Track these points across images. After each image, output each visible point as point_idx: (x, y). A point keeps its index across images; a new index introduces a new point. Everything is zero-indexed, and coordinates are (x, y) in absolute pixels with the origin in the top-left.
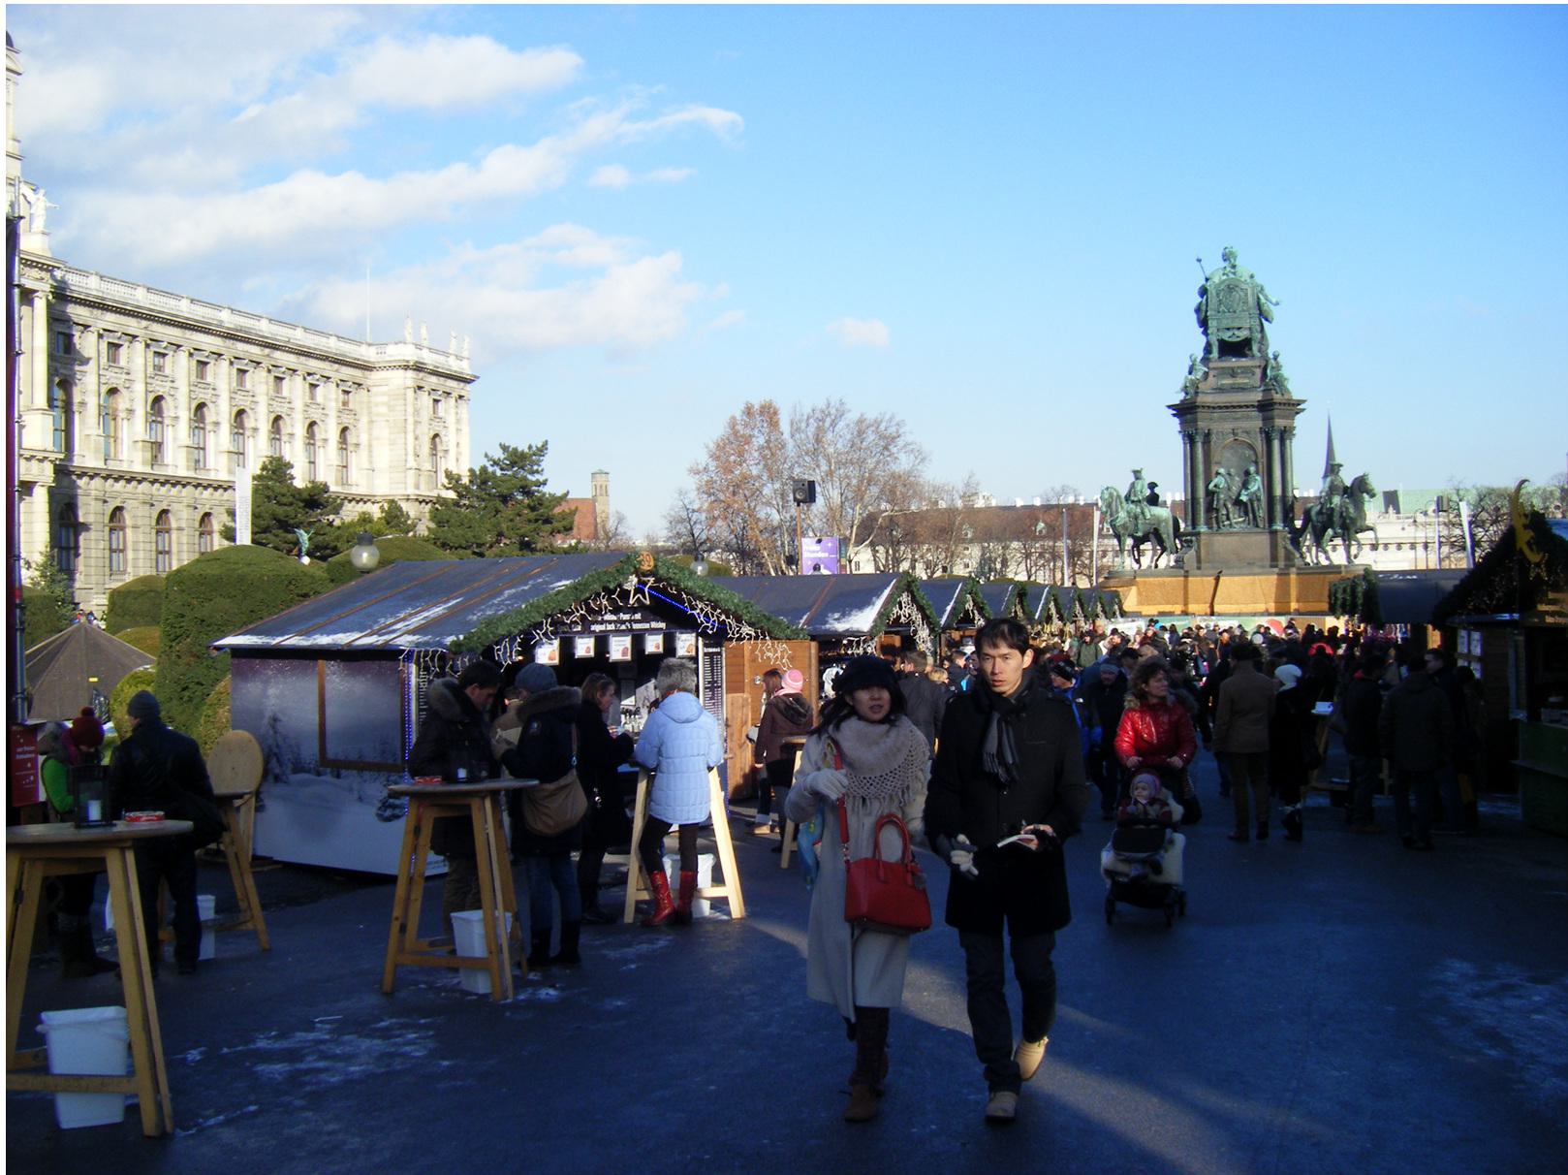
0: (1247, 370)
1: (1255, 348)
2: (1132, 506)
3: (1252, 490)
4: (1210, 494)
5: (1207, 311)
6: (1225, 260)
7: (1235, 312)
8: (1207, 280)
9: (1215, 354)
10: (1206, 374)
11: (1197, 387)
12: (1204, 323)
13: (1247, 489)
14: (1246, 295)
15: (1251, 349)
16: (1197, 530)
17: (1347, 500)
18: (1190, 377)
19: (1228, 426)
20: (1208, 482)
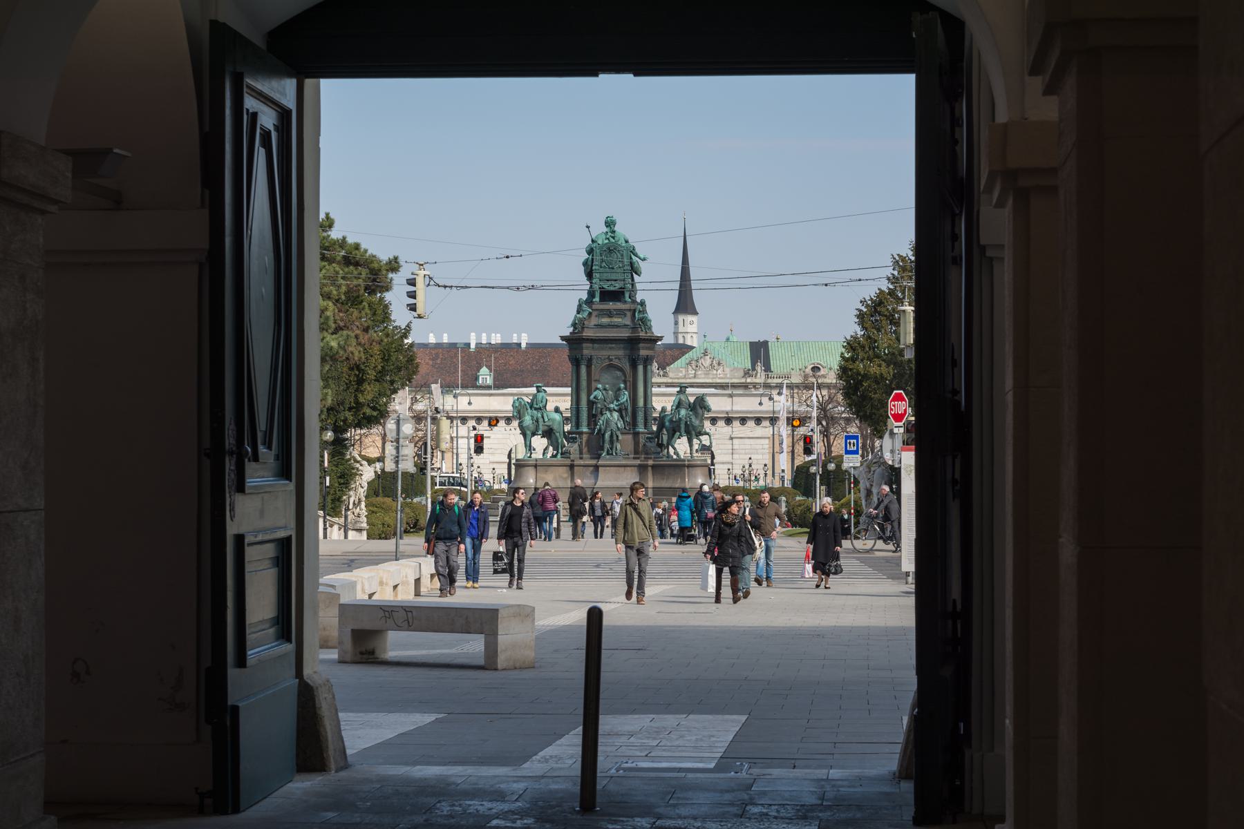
0: (621, 313)
1: (627, 295)
2: (535, 412)
3: (622, 401)
4: (591, 404)
5: (592, 266)
6: (607, 227)
7: (613, 268)
8: (593, 241)
9: (597, 299)
10: (590, 314)
11: (584, 324)
12: (589, 275)
13: (618, 400)
14: (622, 255)
15: (624, 297)
16: (580, 430)
17: (691, 413)
18: (578, 315)
19: (605, 353)
20: (589, 394)
